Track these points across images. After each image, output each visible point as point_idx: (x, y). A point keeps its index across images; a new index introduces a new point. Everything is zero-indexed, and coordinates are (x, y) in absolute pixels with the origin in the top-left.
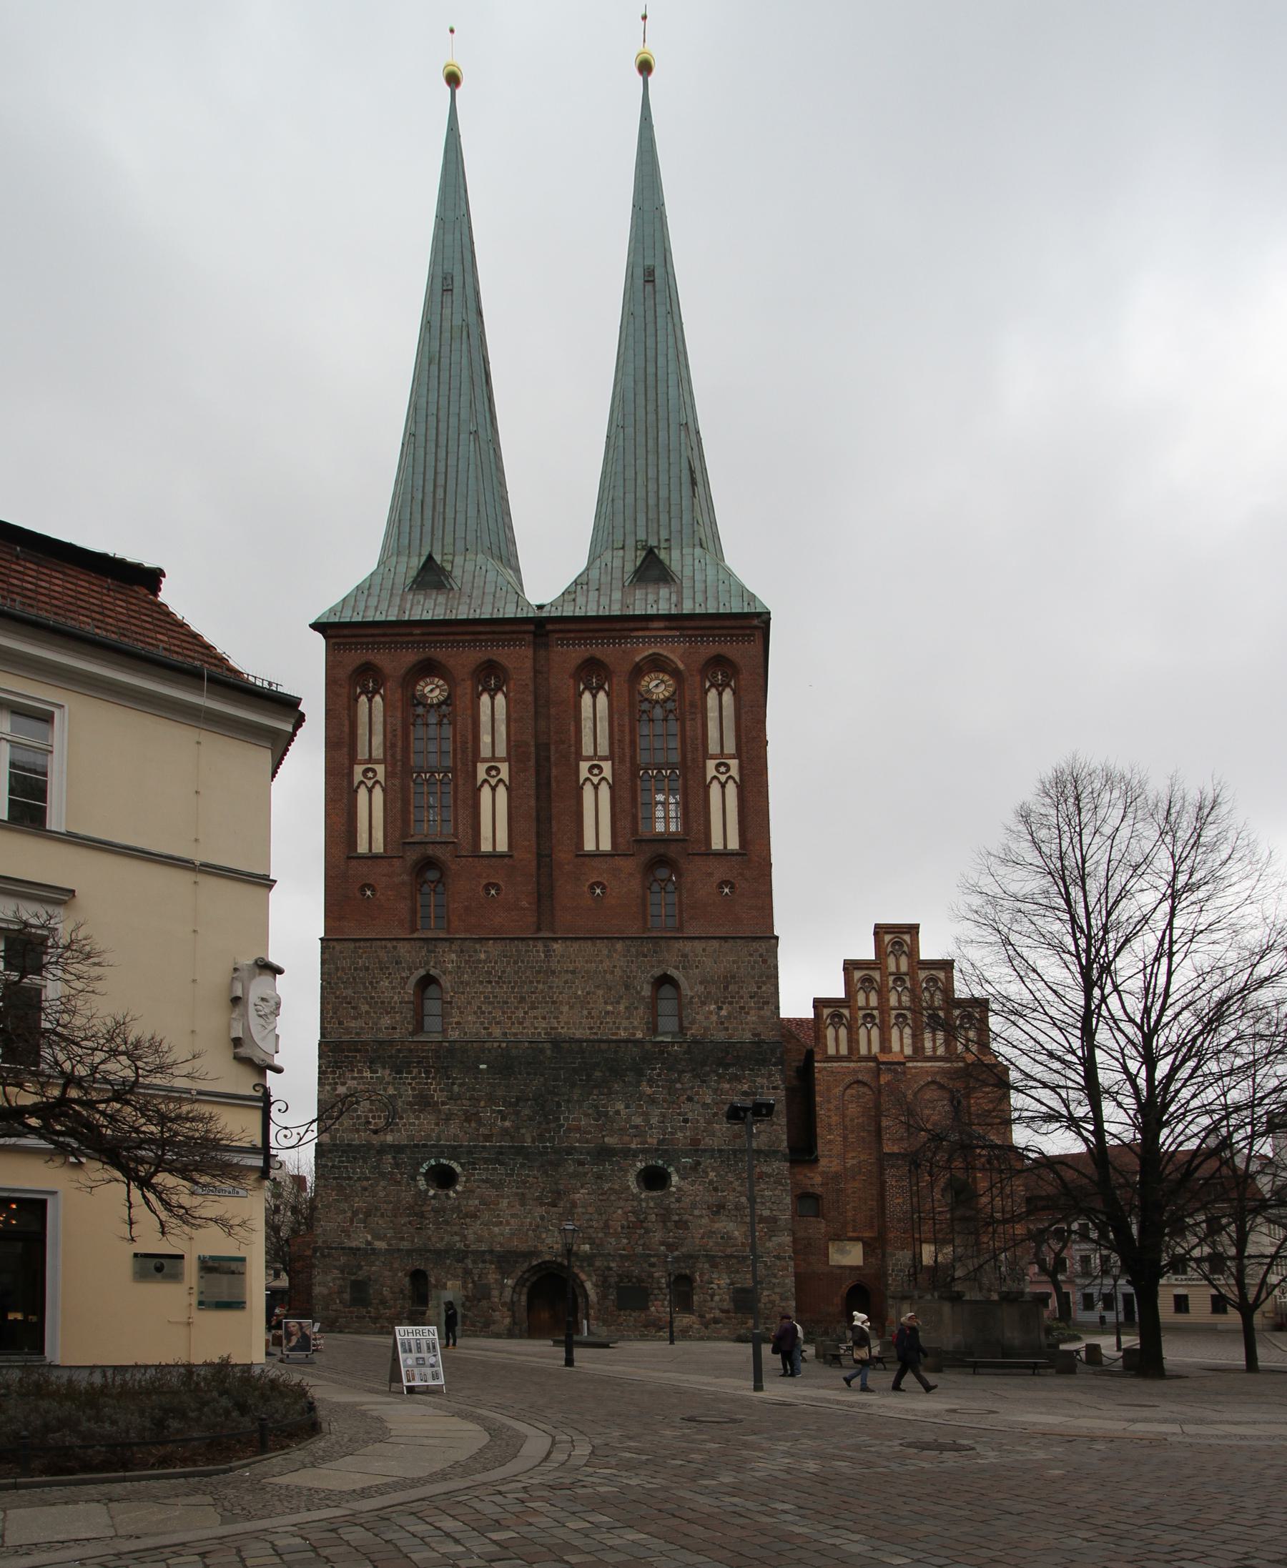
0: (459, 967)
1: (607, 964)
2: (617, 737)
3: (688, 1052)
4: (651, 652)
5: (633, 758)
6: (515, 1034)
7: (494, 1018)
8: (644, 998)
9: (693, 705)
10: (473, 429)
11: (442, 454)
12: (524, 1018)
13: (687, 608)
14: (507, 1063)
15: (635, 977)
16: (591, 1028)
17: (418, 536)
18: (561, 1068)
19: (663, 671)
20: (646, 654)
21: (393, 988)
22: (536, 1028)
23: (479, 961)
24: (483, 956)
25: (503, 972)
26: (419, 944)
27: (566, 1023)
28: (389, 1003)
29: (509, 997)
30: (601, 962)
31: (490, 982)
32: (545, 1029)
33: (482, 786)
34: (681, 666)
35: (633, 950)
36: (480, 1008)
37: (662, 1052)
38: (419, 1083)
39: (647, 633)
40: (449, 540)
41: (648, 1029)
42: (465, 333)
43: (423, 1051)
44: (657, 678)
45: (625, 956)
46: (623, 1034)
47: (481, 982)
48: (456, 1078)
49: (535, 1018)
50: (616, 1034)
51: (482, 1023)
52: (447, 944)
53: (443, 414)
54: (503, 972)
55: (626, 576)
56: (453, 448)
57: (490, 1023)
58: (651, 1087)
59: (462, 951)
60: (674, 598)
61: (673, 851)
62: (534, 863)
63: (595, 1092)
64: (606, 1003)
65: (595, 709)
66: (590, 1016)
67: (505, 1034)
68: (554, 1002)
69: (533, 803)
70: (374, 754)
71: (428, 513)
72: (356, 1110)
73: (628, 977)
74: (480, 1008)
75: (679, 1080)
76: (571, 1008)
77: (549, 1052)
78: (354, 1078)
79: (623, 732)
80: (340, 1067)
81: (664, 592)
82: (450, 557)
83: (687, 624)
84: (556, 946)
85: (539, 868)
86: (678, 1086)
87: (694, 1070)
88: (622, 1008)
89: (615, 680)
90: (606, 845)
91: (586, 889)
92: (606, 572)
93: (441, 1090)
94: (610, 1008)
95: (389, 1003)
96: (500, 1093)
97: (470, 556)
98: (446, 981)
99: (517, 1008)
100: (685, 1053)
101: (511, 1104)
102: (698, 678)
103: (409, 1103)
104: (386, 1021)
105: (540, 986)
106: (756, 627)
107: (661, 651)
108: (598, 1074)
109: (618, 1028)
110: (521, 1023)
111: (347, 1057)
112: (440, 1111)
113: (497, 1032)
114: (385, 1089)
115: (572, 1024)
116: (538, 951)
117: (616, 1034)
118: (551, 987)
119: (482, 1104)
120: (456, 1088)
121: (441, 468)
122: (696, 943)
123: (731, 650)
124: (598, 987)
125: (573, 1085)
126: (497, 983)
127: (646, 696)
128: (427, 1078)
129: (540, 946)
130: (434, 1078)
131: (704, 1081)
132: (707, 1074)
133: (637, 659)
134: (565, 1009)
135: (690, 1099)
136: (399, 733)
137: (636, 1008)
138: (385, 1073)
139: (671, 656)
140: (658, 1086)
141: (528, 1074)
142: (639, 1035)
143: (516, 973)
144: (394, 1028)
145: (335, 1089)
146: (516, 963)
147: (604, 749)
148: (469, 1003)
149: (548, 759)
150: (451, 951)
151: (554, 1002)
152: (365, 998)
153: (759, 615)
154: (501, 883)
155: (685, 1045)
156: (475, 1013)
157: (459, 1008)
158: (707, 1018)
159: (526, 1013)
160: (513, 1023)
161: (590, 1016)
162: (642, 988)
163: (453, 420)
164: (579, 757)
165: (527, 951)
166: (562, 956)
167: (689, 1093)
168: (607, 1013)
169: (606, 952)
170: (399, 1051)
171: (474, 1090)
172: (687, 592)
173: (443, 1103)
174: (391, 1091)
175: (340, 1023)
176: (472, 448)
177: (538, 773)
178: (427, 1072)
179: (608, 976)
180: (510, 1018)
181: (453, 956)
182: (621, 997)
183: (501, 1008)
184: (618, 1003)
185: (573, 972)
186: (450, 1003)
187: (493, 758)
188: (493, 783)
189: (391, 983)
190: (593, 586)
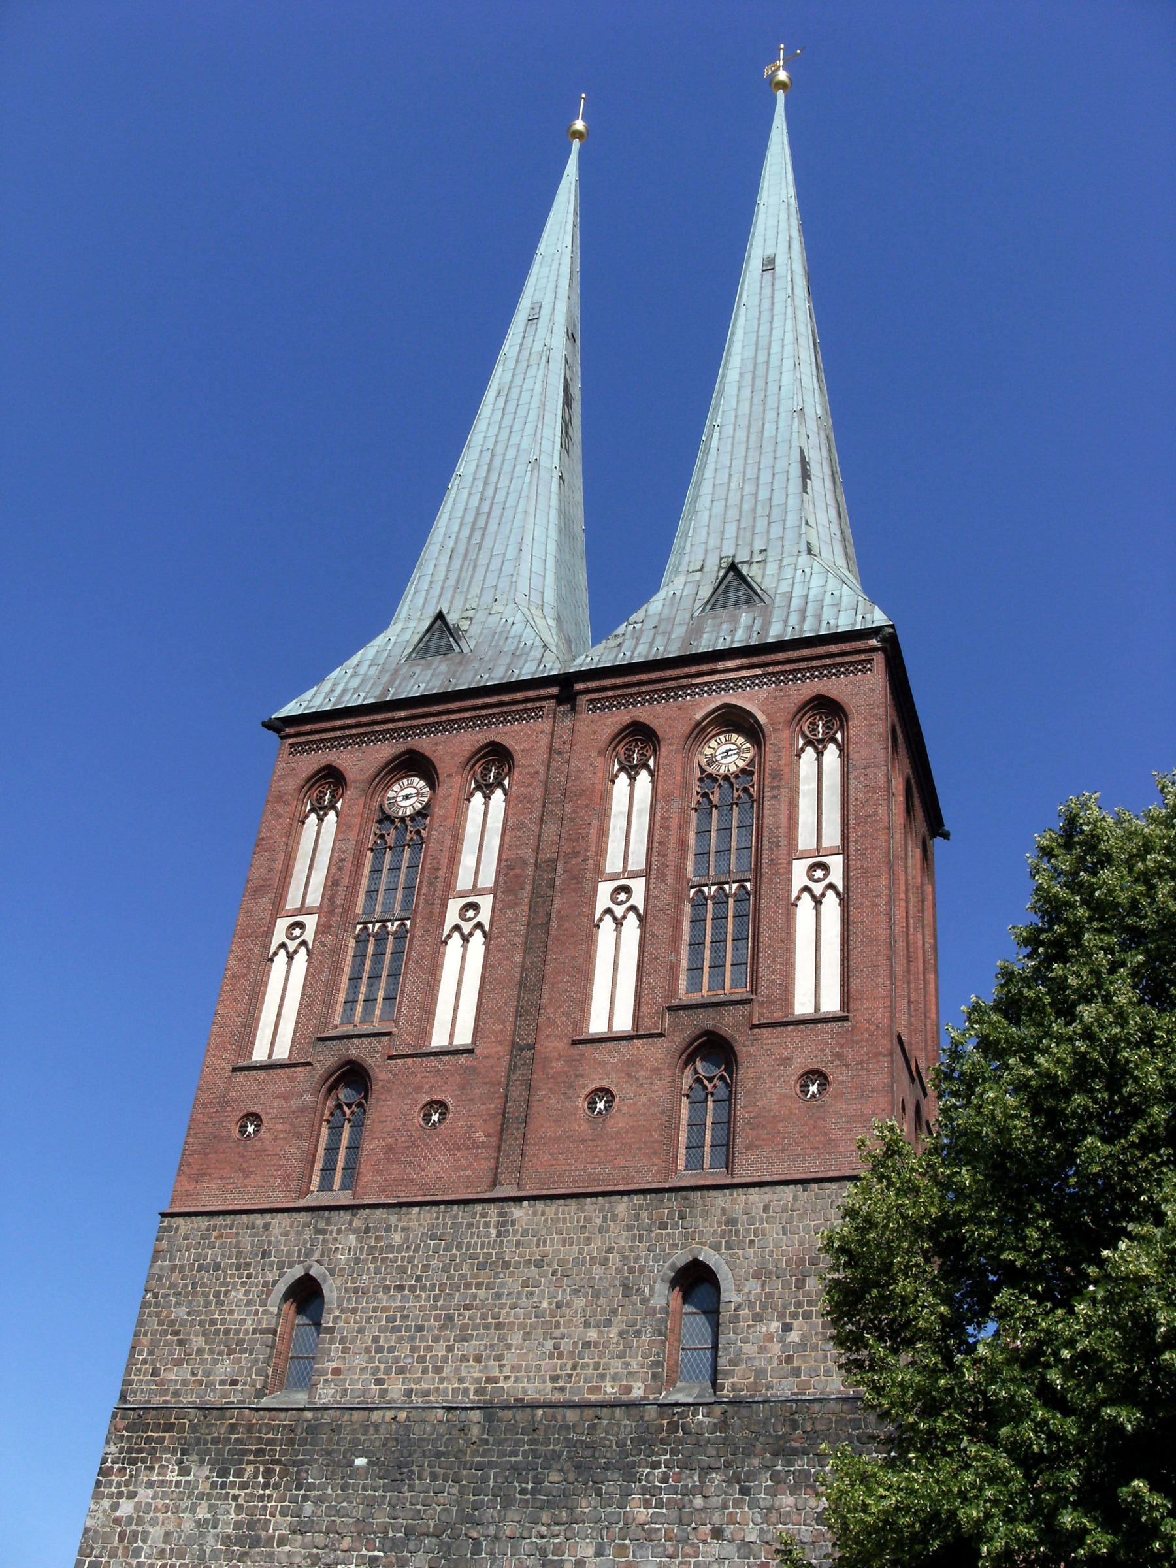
0: (357, 1261)
1: (598, 1244)
2: (657, 838)
3: (723, 1425)
4: (719, 703)
5: (681, 869)
6: (426, 1393)
7: (396, 1360)
8: (654, 1309)
9: (776, 775)
10: (532, 458)
11: (490, 491)
12: (445, 1359)
13: (774, 633)
14: (400, 1453)
15: (642, 1270)
16: (555, 1379)
17: (437, 593)
18: (491, 1465)
19: (739, 730)
20: (713, 706)
21: (249, 1303)
22: (461, 1380)
23: (391, 1247)
24: (398, 1238)
25: (426, 1267)
26: (304, 1217)
27: (514, 1368)
28: (237, 1332)
29: (426, 1318)
30: (588, 1242)
31: (400, 1288)
32: (477, 1381)
33: (449, 936)
34: (762, 718)
35: (644, 1214)
36: (376, 1339)
37: (674, 1427)
38: (251, 1497)
39: (716, 677)
40: (475, 590)
41: (655, 1376)
42: (544, 358)
43: (271, 1428)
44: (728, 741)
45: (629, 1228)
46: (610, 1390)
47: (387, 1289)
48: (311, 1487)
49: (464, 1358)
50: (597, 1389)
51: (376, 1370)
52: (347, 1216)
53: (499, 450)
54: (426, 1267)
55: (698, 604)
56: (503, 483)
57: (387, 1372)
58: (647, 1505)
59: (367, 1230)
60: (756, 628)
61: (727, 1023)
62: (505, 1062)
63: (545, 1517)
64: (587, 1325)
65: (630, 801)
66: (557, 1353)
67: (408, 1393)
68: (499, 1326)
69: (518, 957)
70: (308, 903)
71: (456, 564)
72: (137, 1553)
73: (631, 1270)
74: (376, 1339)
75: (700, 1491)
76: (527, 1336)
77: (475, 1431)
78: (150, 1485)
79: (667, 828)
80: (133, 1462)
81: (744, 618)
82: (470, 614)
83: (773, 657)
84: (518, 1213)
85: (513, 1068)
86: (698, 1502)
87: (728, 1466)
88: (613, 1333)
89: (664, 751)
90: (624, 1023)
91: (582, 1103)
92: (672, 604)
93: (283, 1514)
94: (593, 1335)
95: (237, 1332)
96: (381, 1518)
97: (498, 607)
98: (331, 1290)
99: (436, 1339)
100: (715, 1428)
101: (395, 1545)
102: (785, 734)
103: (226, 1540)
104: (225, 1368)
105: (482, 1294)
106: (874, 649)
107: (734, 702)
108: (555, 1477)
109: (602, 1377)
110: (438, 1370)
111: (149, 1440)
112: (271, 1555)
113: (396, 1389)
114: (193, 1511)
115: (527, 1372)
116: (487, 1225)
117: (598, 1388)
118: (498, 1296)
119: (347, 1543)
120: (308, 1507)
121: (485, 508)
122: (754, 1195)
123: (835, 687)
124: (575, 1292)
125: (507, 1503)
126: (413, 1289)
127: (709, 770)
128: (266, 1486)
129: (492, 1210)
130: (276, 1486)
131: (744, 1491)
132: (750, 1476)
133: (698, 717)
134: (516, 1338)
135: (717, 1533)
136: (348, 864)
137: (638, 1333)
138: (201, 1474)
139: (748, 707)
140: (660, 1505)
141: (434, 1477)
142: (638, 1392)
143: (445, 1268)
144: (234, 1383)
145: (115, 1507)
146: (448, 1249)
147: (638, 861)
148: (361, 1331)
149: (551, 884)
150: (351, 1229)
151: (499, 1326)
152: (201, 1323)
153: (875, 631)
154: (449, 1101)
155: (718, 1410)
156: (367, 1350)
157: (343, 1340)
158: (762, 1350)
159: (449, 1349)
160: (425, 1371)
161: (557, 1353)
162: (652, 1289)
163: (511, 453)
164: (599, 874)
165: (470, 1225)
166: (525, 1233)
167: (716, 1518)
168: (587, 1344)
169: (599, 1221)
170: (233, 1428)
171: (338, 1513)
172: (777, 615)
173: (282, 1541)
174: (202, 1513)
175: (155, 1373)
176: (527, 480)
177: (533, 908)
178: (268, 1473)
179: (598, 1270)
180: (421, 1359)
181: (352, 1238)
182: (614, 1312)
183: (412, 1339)
184: (608, 1323)
185: (539, 1264)
186: (331, 1330)
187: (475, 891)
188: (466, 931)
189: (246, 1293)
190: (649, 624)
